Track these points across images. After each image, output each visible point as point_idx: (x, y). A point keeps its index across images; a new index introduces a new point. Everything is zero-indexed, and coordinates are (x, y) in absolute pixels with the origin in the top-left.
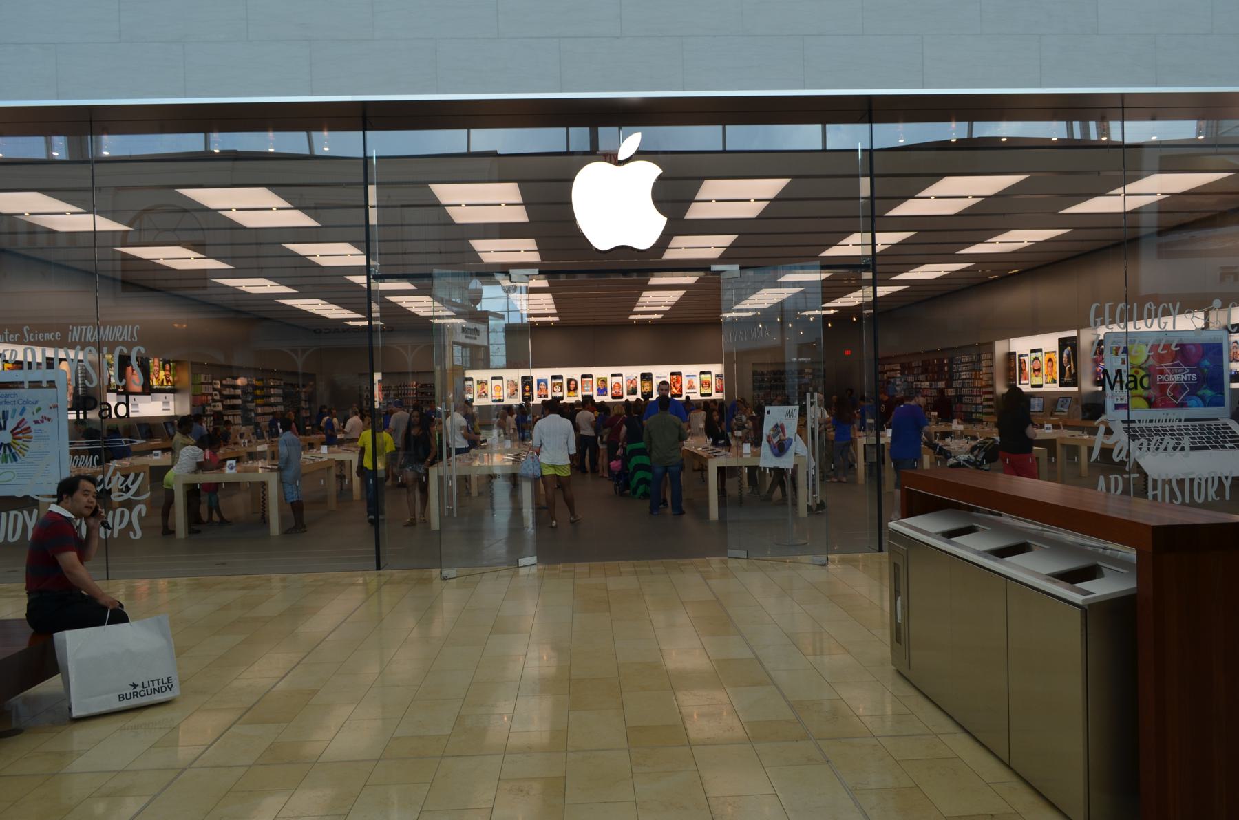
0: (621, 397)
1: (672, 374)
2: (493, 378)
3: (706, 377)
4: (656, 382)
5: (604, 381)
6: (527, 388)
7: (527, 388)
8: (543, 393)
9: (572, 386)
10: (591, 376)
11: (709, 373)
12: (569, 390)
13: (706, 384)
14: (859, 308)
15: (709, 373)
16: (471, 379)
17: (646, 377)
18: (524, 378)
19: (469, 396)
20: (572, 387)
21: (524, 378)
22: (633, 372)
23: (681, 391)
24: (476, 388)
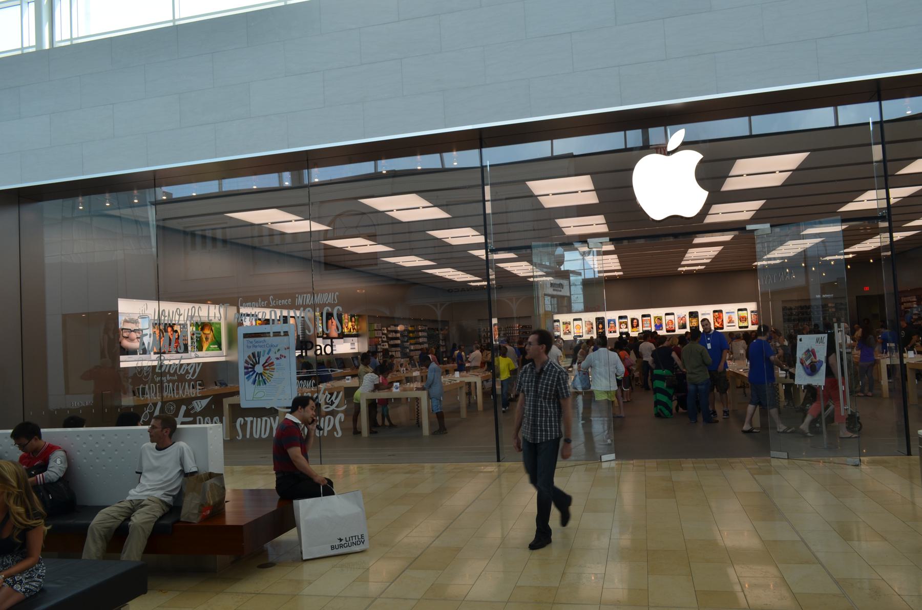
0: (674, 331)
1: (715, 312)
2: (575, 320)
3: (743, 313)
5: (660, 319)
6: (601, 326)
7: (601, 326)
8: (613, 330)
9: (635, 323)
10: (649, 316)
11: (746, 310)
12: (633, 327)
14: (877, 250)
15: (746, 310)
16: (558, 321)
17: (693, 315)
18: (598, 319)
19: (557, 334)
20: (635, 324)
21: (598, 319)
22: (682, 312)
23: (722, 325)
24: (562, 327)
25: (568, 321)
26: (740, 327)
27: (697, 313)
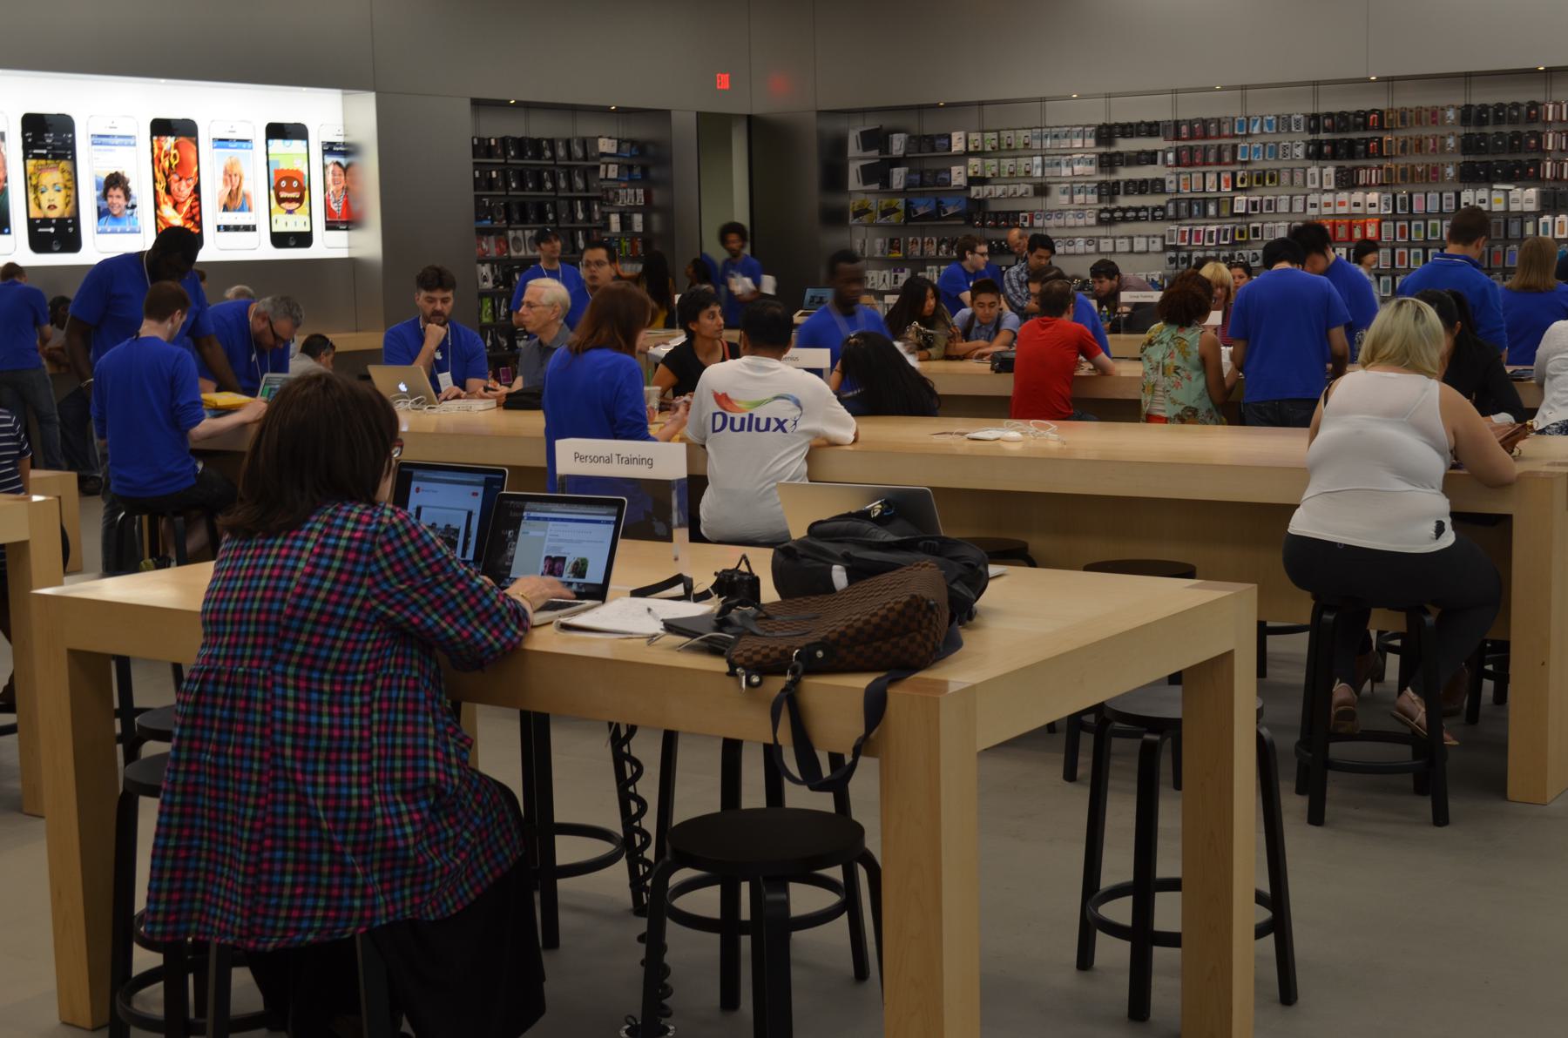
1: (161, 127)
3: (288, 154)
4: (92, 165)
13: (287, 189)
23: (195, 216)
26: (280, 240)
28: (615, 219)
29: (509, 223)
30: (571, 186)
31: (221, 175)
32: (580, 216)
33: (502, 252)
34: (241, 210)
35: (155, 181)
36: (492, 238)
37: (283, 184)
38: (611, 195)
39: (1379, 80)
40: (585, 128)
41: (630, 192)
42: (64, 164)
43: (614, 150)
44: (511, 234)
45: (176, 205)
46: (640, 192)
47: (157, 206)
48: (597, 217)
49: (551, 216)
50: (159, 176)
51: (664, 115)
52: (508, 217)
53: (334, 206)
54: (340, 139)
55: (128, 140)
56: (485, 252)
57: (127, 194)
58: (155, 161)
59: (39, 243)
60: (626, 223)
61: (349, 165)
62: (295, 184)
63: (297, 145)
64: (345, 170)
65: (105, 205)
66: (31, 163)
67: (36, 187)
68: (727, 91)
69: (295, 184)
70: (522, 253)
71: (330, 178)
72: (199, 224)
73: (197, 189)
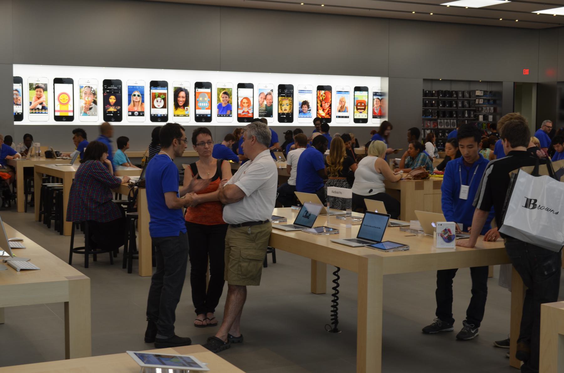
1: (320, 88)
2: (58, 81)
3: (361, 96)
4: (298, 98)
5: (227, 93)
6: (112, 99)
7: (112, 99)
8: (137, 109)
9: (181, 100)
10: (208, 85)
11: (365, 89)
12: (177, 106)
15: (365, 89)
16: (19, 80)
17: (285, 91)
18: (107, 83)
19: (17, 109)
20: (181, 100)
21: (107, 83)
22: (267, 82)
23: (329, 113)
25: (41, 82)
26: (356, 121)
27: (291, 87)
28: (481, 118)
29: (438, 117)
30: (463, 106)
31: (338, 101)
32: (466, 115)
33: (435, 126)
34: (345, 112)
35: (317, 103)
36: (432, 122)
37: (359, 104)
38: (480, 109)
39: (482, 82)
40: (472, 87)
41: (488, 108)
42: (290, 98)
43: (482, 95)
44: (439, 121)
45: (323, 110)
46: (492, 108)
47: (317, 110)
48: (472, 116)
49: (455, 116)
50: (319, 102)
51: (501, 83)
52: (438, 116)
53: (376, 111)
54: (379, 91)
55: (310, 92)
56: (428, 126)
57: (308, 107)
58: (318, 98)
59: (281, 119)
60: (486, 118)
61: (382, 99)
62: (363, 104)
63: (364, 93)
64: (381, 100)
65: (301, 110)
66: (280, 98)
67: (281, 105)
68: (527, 75)
69: (363, 104)
70: (443, 127)
71: (375, 103)
72: (330, 116)
73: (330, 106)
